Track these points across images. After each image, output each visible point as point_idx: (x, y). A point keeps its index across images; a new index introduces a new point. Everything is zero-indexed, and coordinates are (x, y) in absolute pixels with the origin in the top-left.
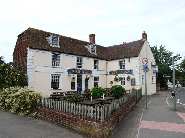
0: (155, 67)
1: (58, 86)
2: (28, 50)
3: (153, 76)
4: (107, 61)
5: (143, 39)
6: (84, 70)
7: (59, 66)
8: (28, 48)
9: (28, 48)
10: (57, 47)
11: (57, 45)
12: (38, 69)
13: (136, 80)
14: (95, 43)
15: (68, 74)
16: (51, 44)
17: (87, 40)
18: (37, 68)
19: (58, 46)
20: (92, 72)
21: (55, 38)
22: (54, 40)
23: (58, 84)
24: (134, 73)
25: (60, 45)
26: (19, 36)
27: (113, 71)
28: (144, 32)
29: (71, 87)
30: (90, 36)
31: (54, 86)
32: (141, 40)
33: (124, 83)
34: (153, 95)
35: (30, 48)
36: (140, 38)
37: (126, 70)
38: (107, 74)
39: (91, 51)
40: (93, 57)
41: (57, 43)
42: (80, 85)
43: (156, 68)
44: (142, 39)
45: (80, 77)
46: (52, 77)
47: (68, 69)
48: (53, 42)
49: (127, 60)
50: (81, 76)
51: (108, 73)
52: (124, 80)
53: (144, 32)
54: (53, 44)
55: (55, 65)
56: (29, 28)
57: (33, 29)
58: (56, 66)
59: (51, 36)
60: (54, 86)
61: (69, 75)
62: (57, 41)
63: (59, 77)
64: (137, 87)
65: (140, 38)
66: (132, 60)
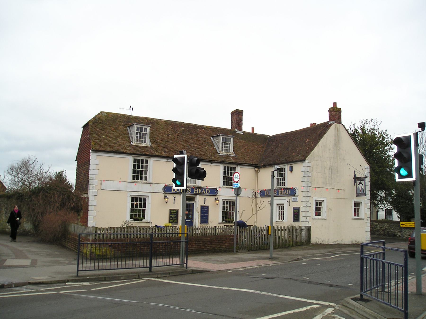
0: (360, 183)
1: (144, 216)
2: (91, 154)
3: (357, 205)
4: (256, 169)
5: (330, 120)
6: (201, 188)
7: (146, 179)
8: (91, 151)
9: (91, 151)
10: (144, 145)
11: (145, 142)
12: (106, 185)
13: (301, 210)
14: (241, 129)
15: (164, 195)
16: (134, 141)
17: (227, 124)
18: (104, 184)
19: (148, 143)
20: (217, 191)
21: (142, 128)
22: (140, 134)
23: (144, 211)
24: (298, 196)
25: (152, 140)
26: (85, 127)
27: (266, 190)
28: (335, 104)
29: (170, 220)
30: (233, 114)
31: (136, 215)
32: (327, 123)
33: (283, 215)
34: (352, 244)
35: (94, 151)
36: (324, 118)
37: (287, 189)
38: (256, 197)
39: (220, 149)
40: (222, 162)
41: (146, 138)
42: (190, 216)
43: (361, 185)
44: (327, 120)
45: (191, 202)
46: (133, 199)
47: (164, 186)
48: (137, 137)
49: (287, 167)
50: (193, 199)
51: (259, 196)
52: (283, 210)
53: (335, 104)
54: (137, 142)
55: (138, 179)
56: (100, 112)
57: (106, 113)
58: (141, 179)
59: (135, 125)
60: (136, 215)
61: (165, 196)
62: (146, 135)
63: (145, 200)
64: (303, 223)
65: (324, 118)
66: (297, 167)
